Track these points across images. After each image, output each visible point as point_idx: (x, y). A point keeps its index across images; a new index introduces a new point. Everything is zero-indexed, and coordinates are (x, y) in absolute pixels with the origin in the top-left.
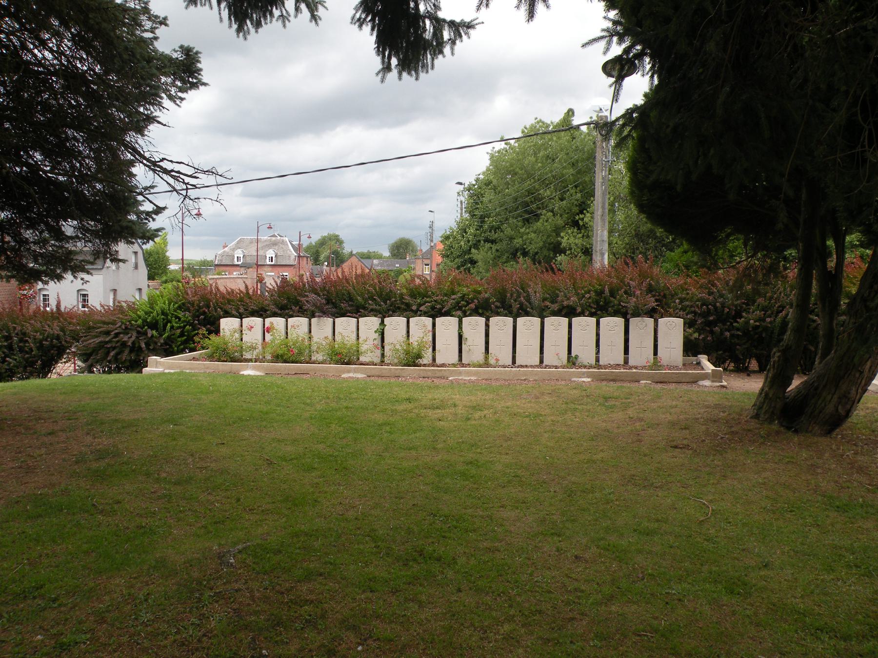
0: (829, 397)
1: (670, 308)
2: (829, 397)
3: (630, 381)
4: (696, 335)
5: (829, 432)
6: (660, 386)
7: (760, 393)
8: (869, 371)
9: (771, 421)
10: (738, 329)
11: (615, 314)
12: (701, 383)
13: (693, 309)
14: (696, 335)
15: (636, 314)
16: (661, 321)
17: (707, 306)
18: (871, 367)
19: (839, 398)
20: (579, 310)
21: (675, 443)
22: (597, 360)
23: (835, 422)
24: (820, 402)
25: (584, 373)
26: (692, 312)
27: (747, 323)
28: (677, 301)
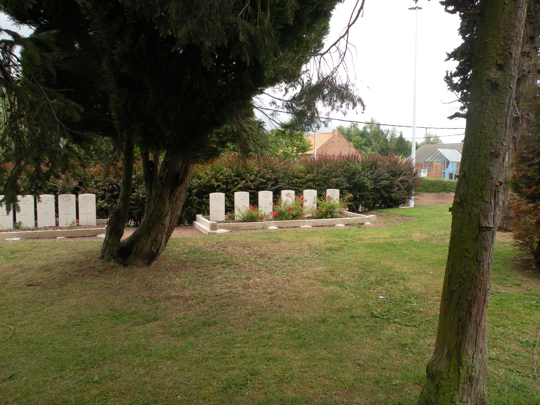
0: (145, 242)
1: (89, 187)
2: (145, 242)
3: (49, 238)
4: (106, 204)
5: (149, 264)
6: (71, 240)
7: (104, 242)
8: (170, 223)
9: (109, 260)
10: (133, 200)
11: (49, 192)
12: (99, 236)
13: (103, 188)
14: (106, 204)
15: (63, 192)
16: (80, 196)
17: (112, 185)
18: (170, 221)
19: (152, 242)
20: (22, 189)
21: (31, 283)
22: (36, 224)
23: (151, 257)
24: (140, 245)
25: (14, 235)
26: (103, 190)
27: (138, 196)
28: (93, 183)
